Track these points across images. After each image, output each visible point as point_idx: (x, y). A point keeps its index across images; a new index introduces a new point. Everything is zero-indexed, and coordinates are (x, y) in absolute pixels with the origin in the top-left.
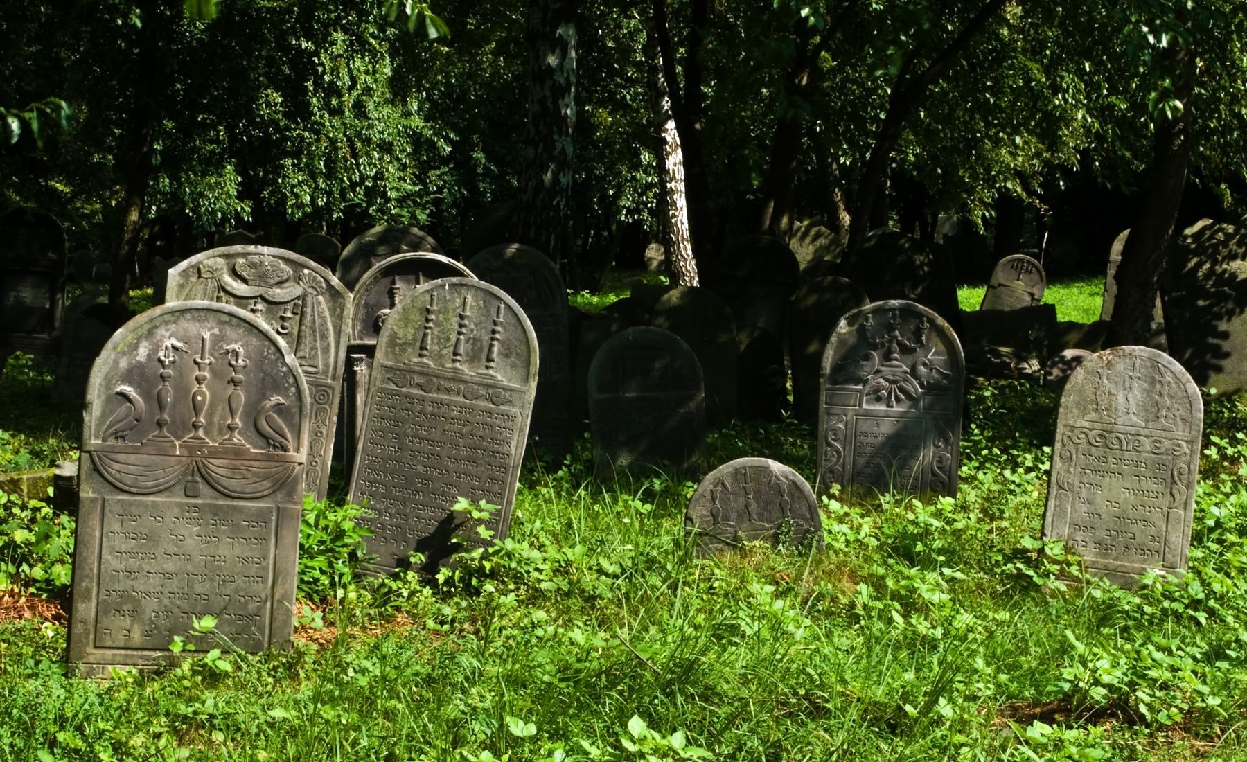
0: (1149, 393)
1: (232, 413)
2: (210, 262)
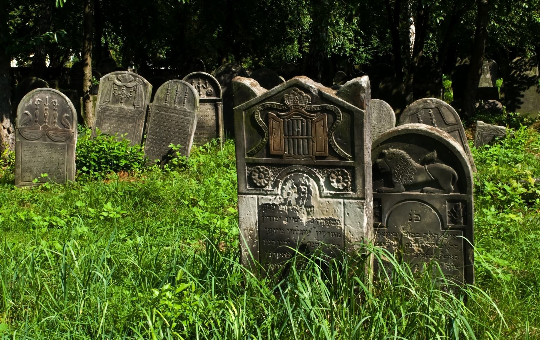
0: (379, 114)
1: (55, 119)
2: (111, 76)
